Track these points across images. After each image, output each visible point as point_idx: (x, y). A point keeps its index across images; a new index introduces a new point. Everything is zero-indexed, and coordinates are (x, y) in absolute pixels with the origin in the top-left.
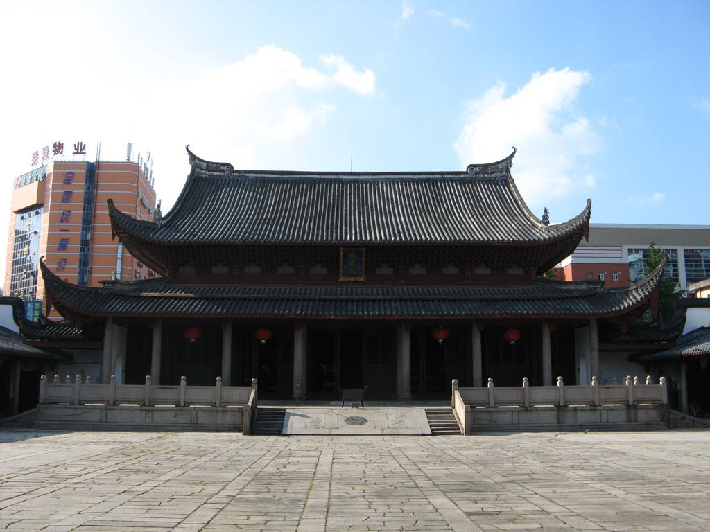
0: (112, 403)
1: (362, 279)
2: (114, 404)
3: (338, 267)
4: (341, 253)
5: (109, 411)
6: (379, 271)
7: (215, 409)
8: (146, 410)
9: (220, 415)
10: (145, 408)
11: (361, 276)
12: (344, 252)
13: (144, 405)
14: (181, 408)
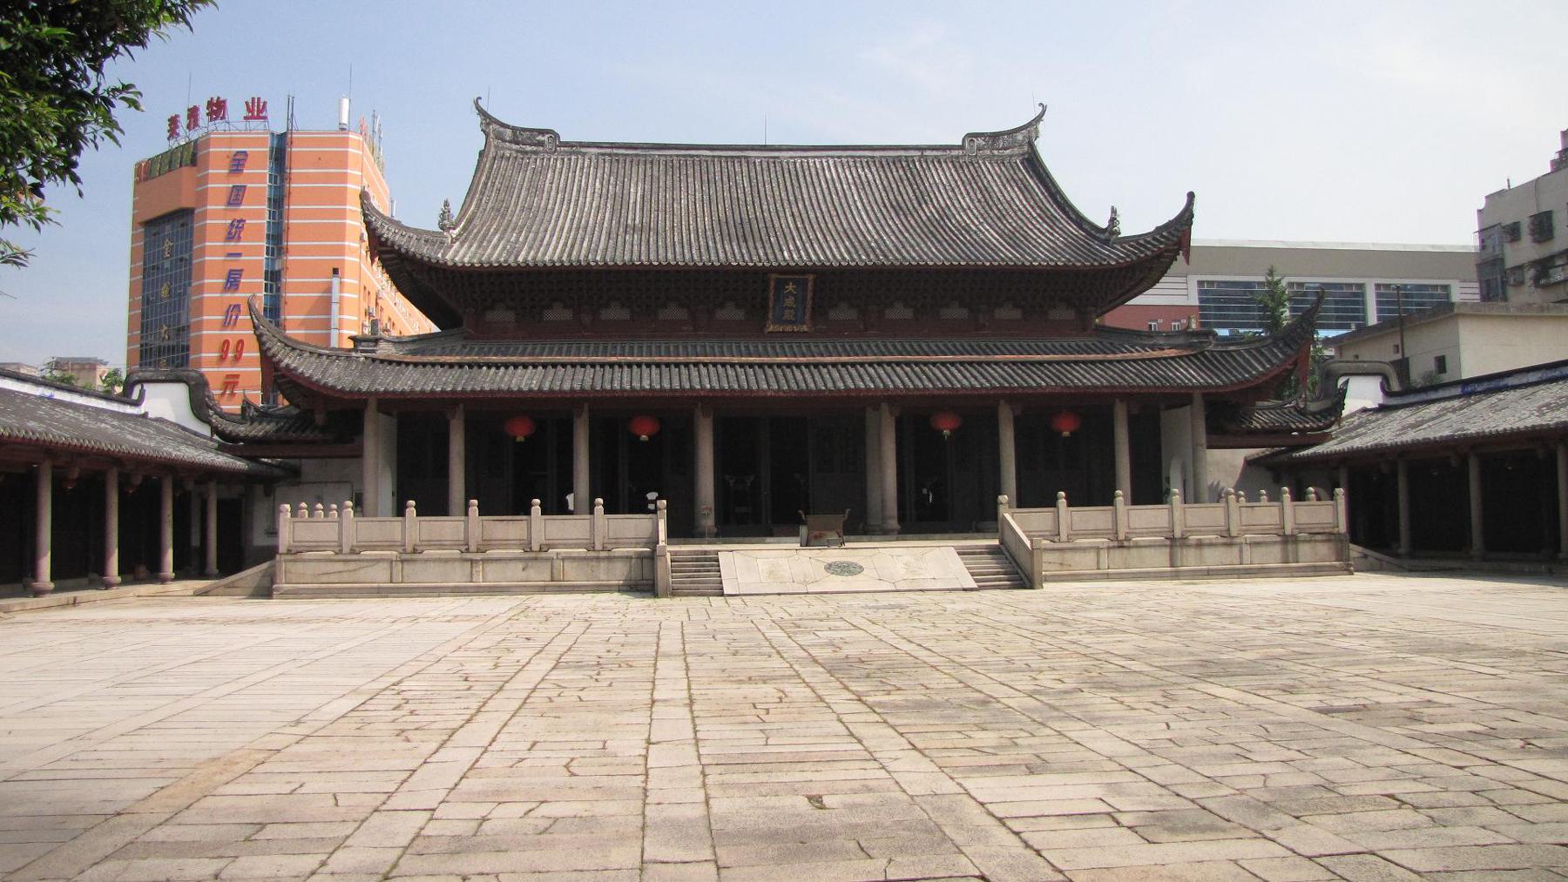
0: (409, 549)
1: (805, 328)
2: (415, 551)
3: (765, 307)
4: (772, 284)
5: (406, 566)
6: (833, 315)
7: (592, 554)
8: (472, 561)
9: (603, 565)
10: (468, 556)
11: (803, 323)
12: (778, 281)
13: (468, 550)
14: (532, 555)
